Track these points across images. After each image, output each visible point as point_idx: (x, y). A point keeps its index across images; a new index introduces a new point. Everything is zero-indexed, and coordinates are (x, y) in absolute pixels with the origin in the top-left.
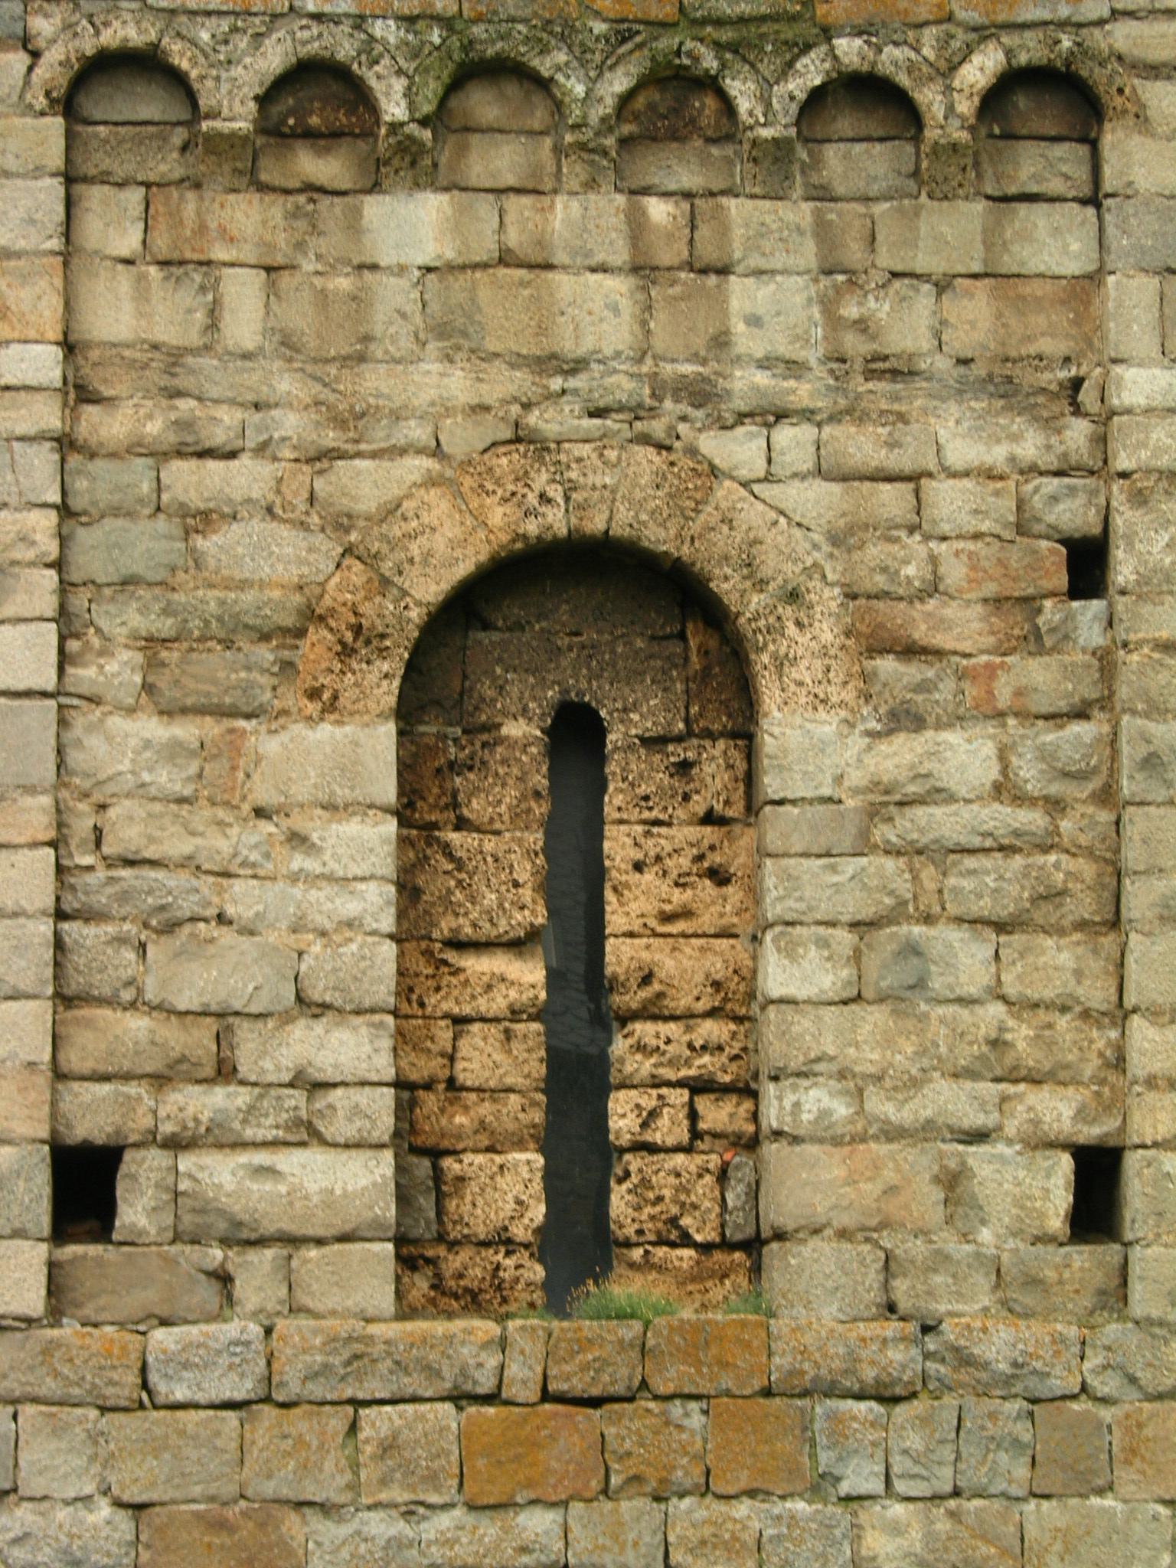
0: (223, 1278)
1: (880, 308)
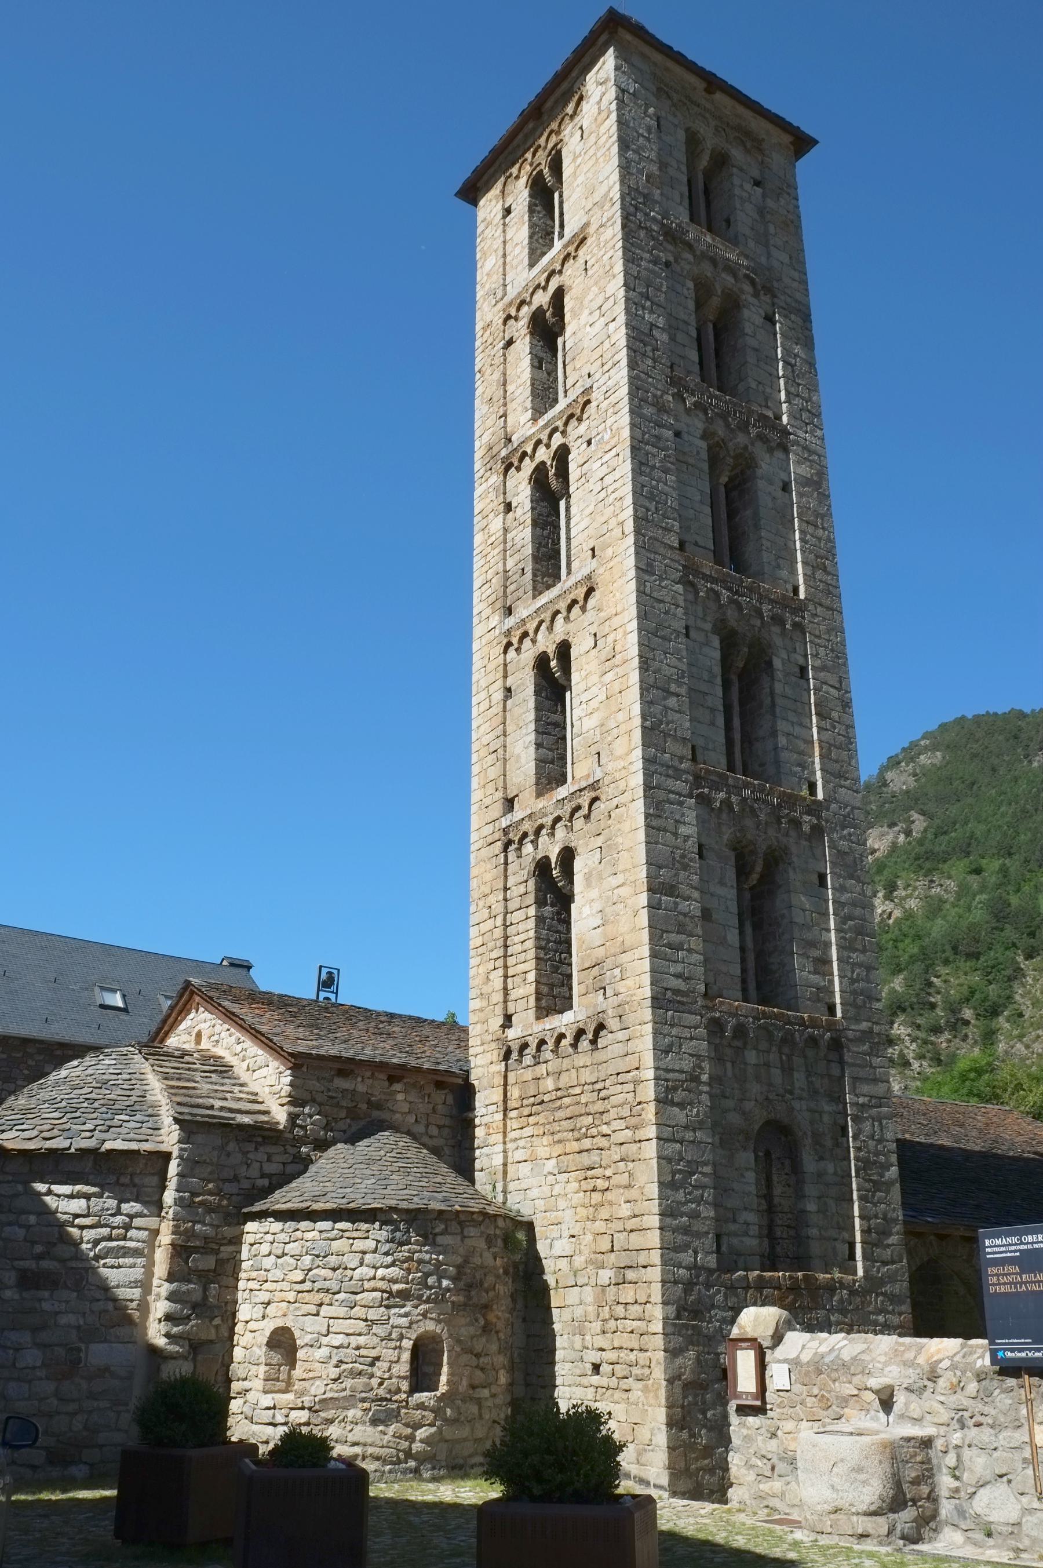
0: (736, 1262)
1: (814, 1079)
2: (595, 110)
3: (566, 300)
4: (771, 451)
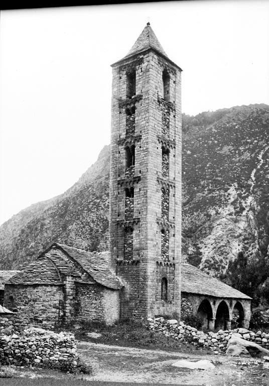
2: (145, 67)
3: (136, 111)
4: (172, 148)
